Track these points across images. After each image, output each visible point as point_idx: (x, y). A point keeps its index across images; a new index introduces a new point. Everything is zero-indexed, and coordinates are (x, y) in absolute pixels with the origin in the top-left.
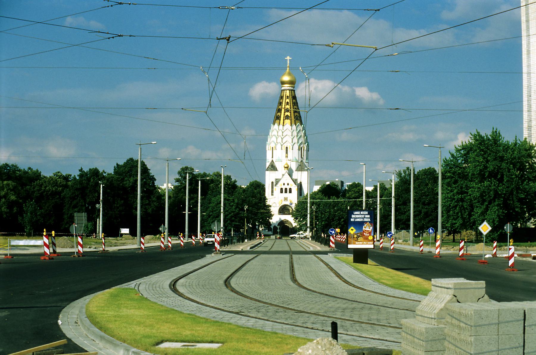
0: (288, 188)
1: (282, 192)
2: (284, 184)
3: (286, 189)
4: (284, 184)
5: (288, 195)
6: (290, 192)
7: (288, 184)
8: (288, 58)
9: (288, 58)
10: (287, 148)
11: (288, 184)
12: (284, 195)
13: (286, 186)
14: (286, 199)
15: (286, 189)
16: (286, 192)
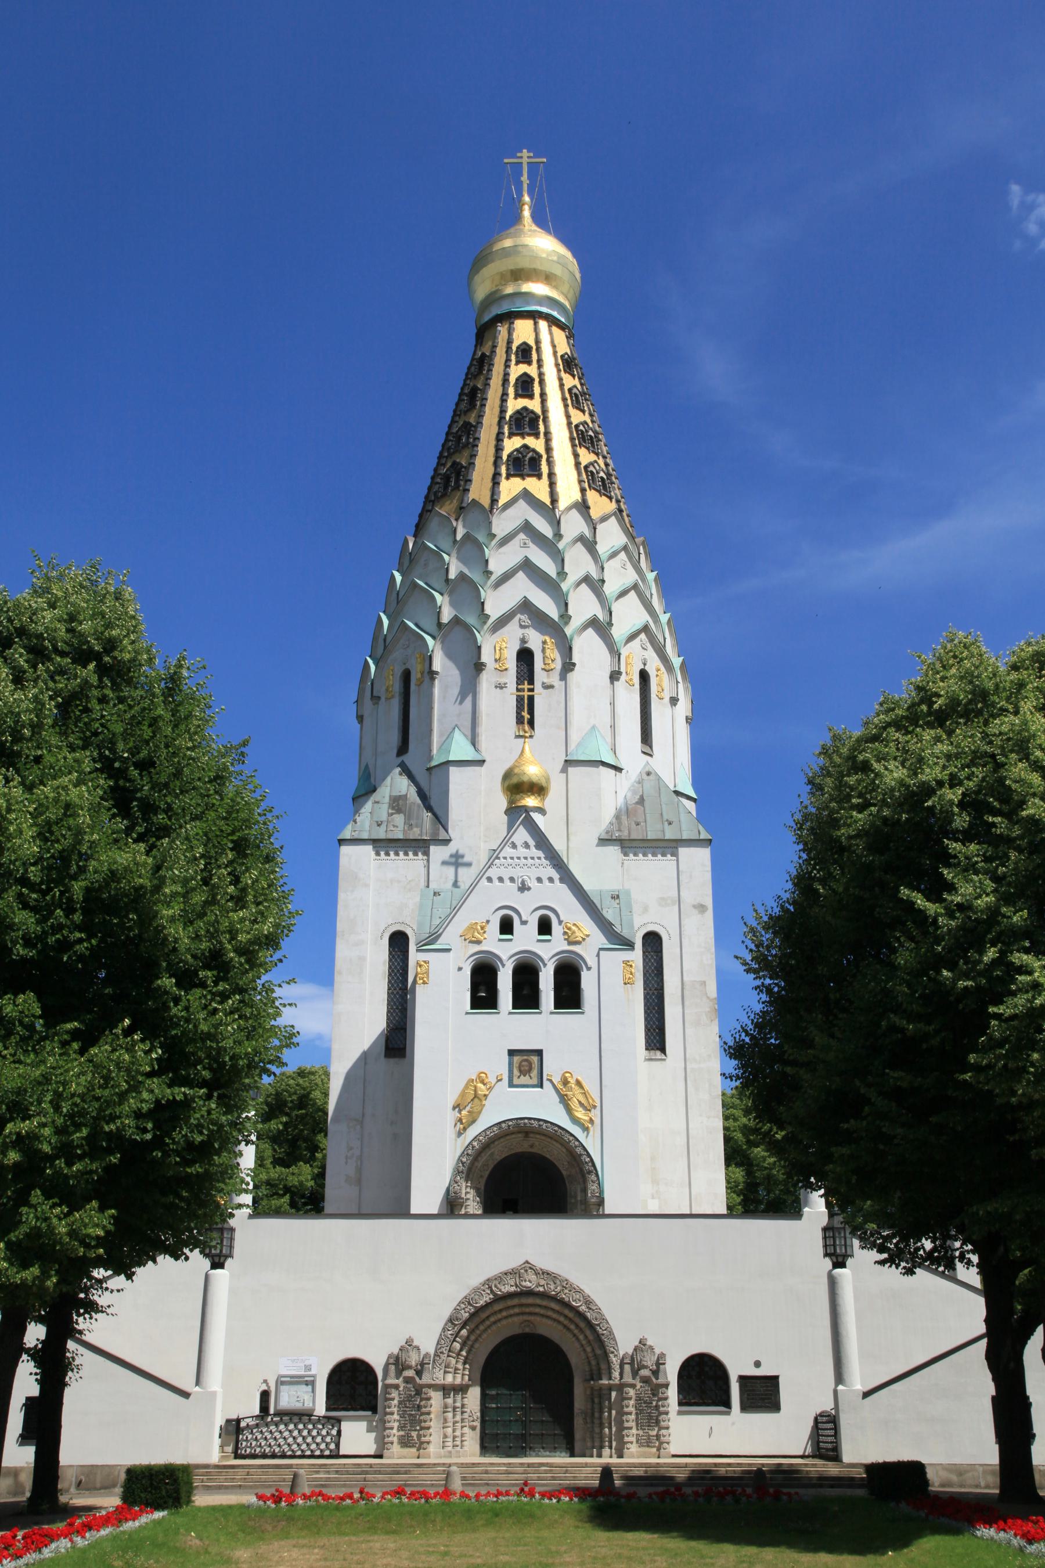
0: (548, 953)
1: (483, 996)
2: (506, 927)
3: (526, 975)
4: (506, 927)
5: (544, 1027)
6: (569, 994)
7: (545, 927)
8: (525, 156)
9: (525, 156)
10: (525, 656)
11: (545, 927)
12: (509, 1026)
13: (526, 938)
14: (526, 1063)
15: (526, 975)
16: (526, 996)
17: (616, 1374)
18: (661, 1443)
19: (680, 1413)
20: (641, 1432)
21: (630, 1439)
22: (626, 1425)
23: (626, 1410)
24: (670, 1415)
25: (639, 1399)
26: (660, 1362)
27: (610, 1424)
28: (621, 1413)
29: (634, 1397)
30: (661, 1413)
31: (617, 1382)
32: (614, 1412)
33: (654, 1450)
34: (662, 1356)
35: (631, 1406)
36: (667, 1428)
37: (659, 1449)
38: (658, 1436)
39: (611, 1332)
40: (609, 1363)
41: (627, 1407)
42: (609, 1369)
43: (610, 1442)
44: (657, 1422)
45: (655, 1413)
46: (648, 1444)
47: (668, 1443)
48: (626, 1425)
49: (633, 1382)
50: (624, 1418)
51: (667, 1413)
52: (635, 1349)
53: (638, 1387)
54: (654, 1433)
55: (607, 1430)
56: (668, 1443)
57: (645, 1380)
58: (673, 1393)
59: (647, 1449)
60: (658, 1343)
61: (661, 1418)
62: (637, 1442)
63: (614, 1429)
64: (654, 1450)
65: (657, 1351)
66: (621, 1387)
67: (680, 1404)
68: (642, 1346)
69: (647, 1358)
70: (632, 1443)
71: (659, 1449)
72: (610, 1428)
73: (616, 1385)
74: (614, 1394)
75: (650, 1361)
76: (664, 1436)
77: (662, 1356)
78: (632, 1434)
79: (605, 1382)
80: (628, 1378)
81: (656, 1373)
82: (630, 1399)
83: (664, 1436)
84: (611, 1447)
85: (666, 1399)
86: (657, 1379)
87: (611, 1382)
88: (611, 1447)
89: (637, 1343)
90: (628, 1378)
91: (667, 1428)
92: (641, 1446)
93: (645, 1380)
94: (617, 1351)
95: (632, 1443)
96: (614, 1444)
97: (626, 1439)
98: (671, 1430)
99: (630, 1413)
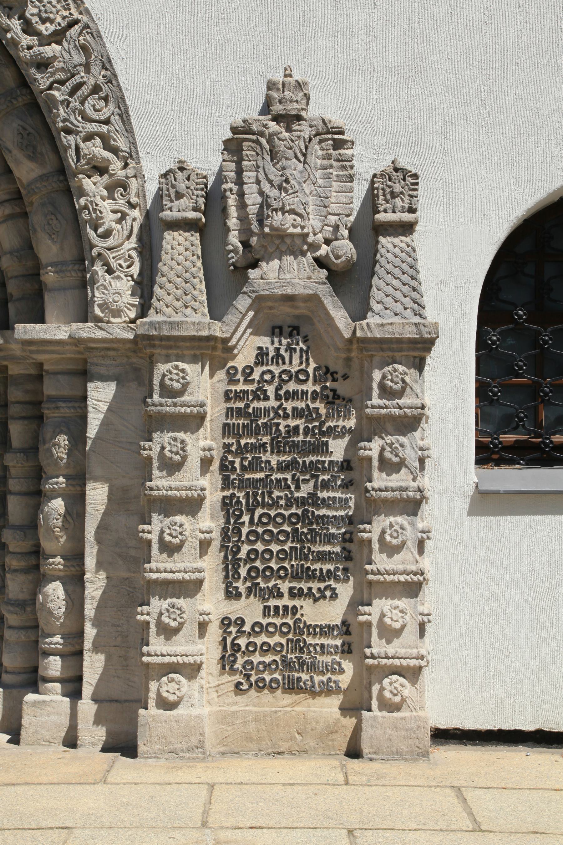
17: (116, 289)
18: (369, 675)
19: (485, 502)
20: (250, 610)
21: (182, 648)
22: (160, 566)
23: (161, 483)
24: (430, 516)
25: (243, 422)
26: (384, 217)
27: (76, 557)
28: (135, 503)
29: (215, 412)
30: (371, 506)
31: (119, 329)
32: (97, 495)
33: (328, 708)
34: (399, 181)
35: (193, 464)
36: (413, 589)
37: (355, 706)
38: (351, 635)
39: (91, 51)
40: (75, 225)
41: (172, 467)
42: (81, 259)
43: (74, 655)
44: (353, 554)
45: (339, 503)
46: (293, 674)
47: (413, 674)
48: (160, 566)
49: (218, 330)
50: (156, 527)
51: (412, 506)
52: (233, 147)
53: (244, 357)
54: (332, 612)
55: (55, 593)
56: (413, 674)
57: (289, 322)
58: (448, 391)
59: (282, 703)
60: (377, 118)
61: (376, 528)
62: (226, 662)
63: (95, 586)
64: (328, 708)
65: (368, 162)
66: (136, 361)
67: (486, 455)
68: (279, 125)
69: (304, 196)
70: (192, 670)
71: (355, 706)
72: (75, 581)
73: (111, 346)
74: (101, 396)
75: (320, 207)
76: (390, 634)
77: (399, 181)
78: (197, 616)
79: (56, 329)
80: (183, 307)
81: (351, 280)
82: (194, 421)
83: (390, 634)
84: (73, 687)
85: (410, 423)
86: (360, 312)
87: (87, 331)
88: (73, 687)
89: (250, 110)
90: (183, 307)
91: (413, 589)
92: (249, 682)
93: (289, 322)
94: (129, 158)
95: (192, 670)
96: (93, 667)
97: (158, 648)
98: (429, 599)
99: (191, 505)
